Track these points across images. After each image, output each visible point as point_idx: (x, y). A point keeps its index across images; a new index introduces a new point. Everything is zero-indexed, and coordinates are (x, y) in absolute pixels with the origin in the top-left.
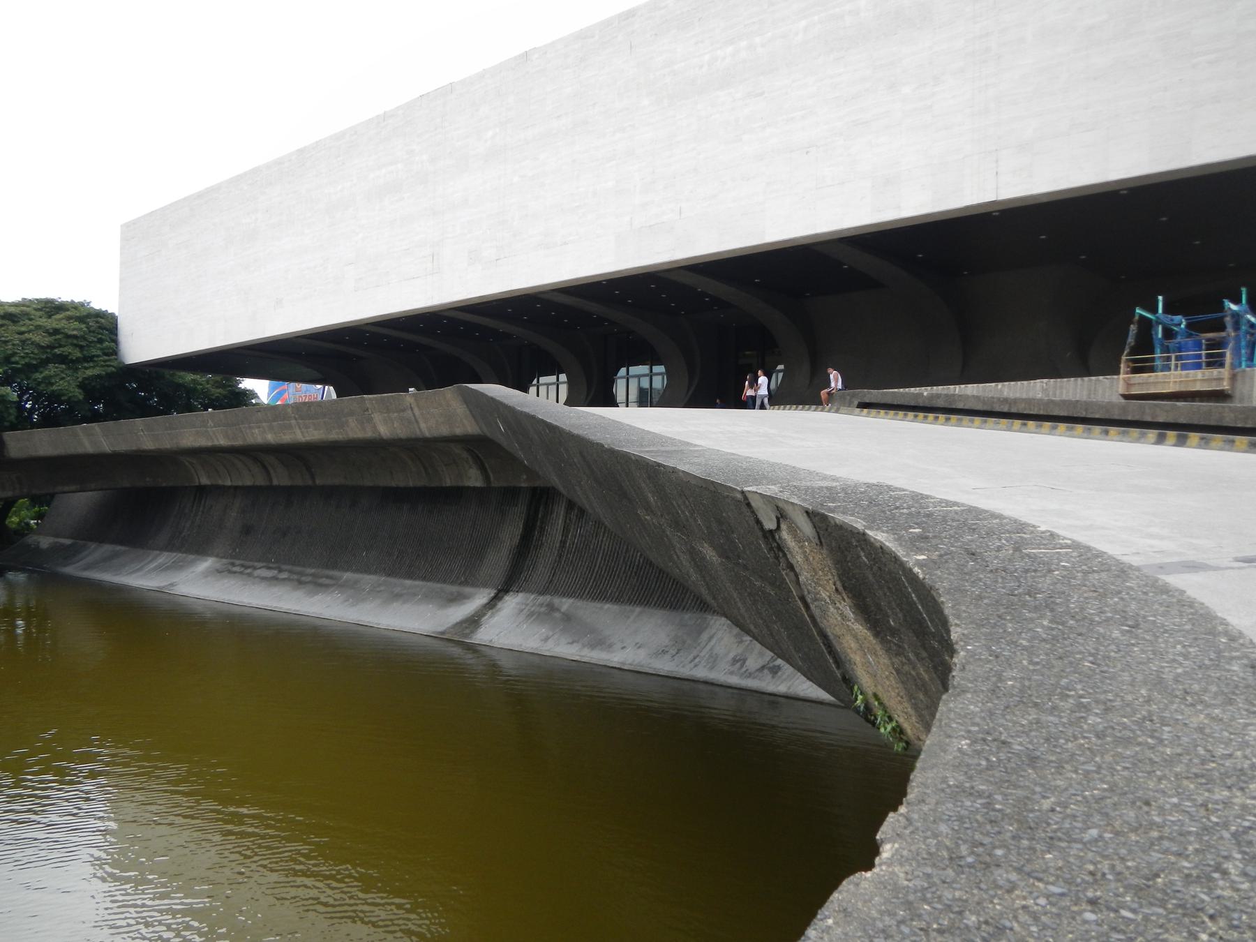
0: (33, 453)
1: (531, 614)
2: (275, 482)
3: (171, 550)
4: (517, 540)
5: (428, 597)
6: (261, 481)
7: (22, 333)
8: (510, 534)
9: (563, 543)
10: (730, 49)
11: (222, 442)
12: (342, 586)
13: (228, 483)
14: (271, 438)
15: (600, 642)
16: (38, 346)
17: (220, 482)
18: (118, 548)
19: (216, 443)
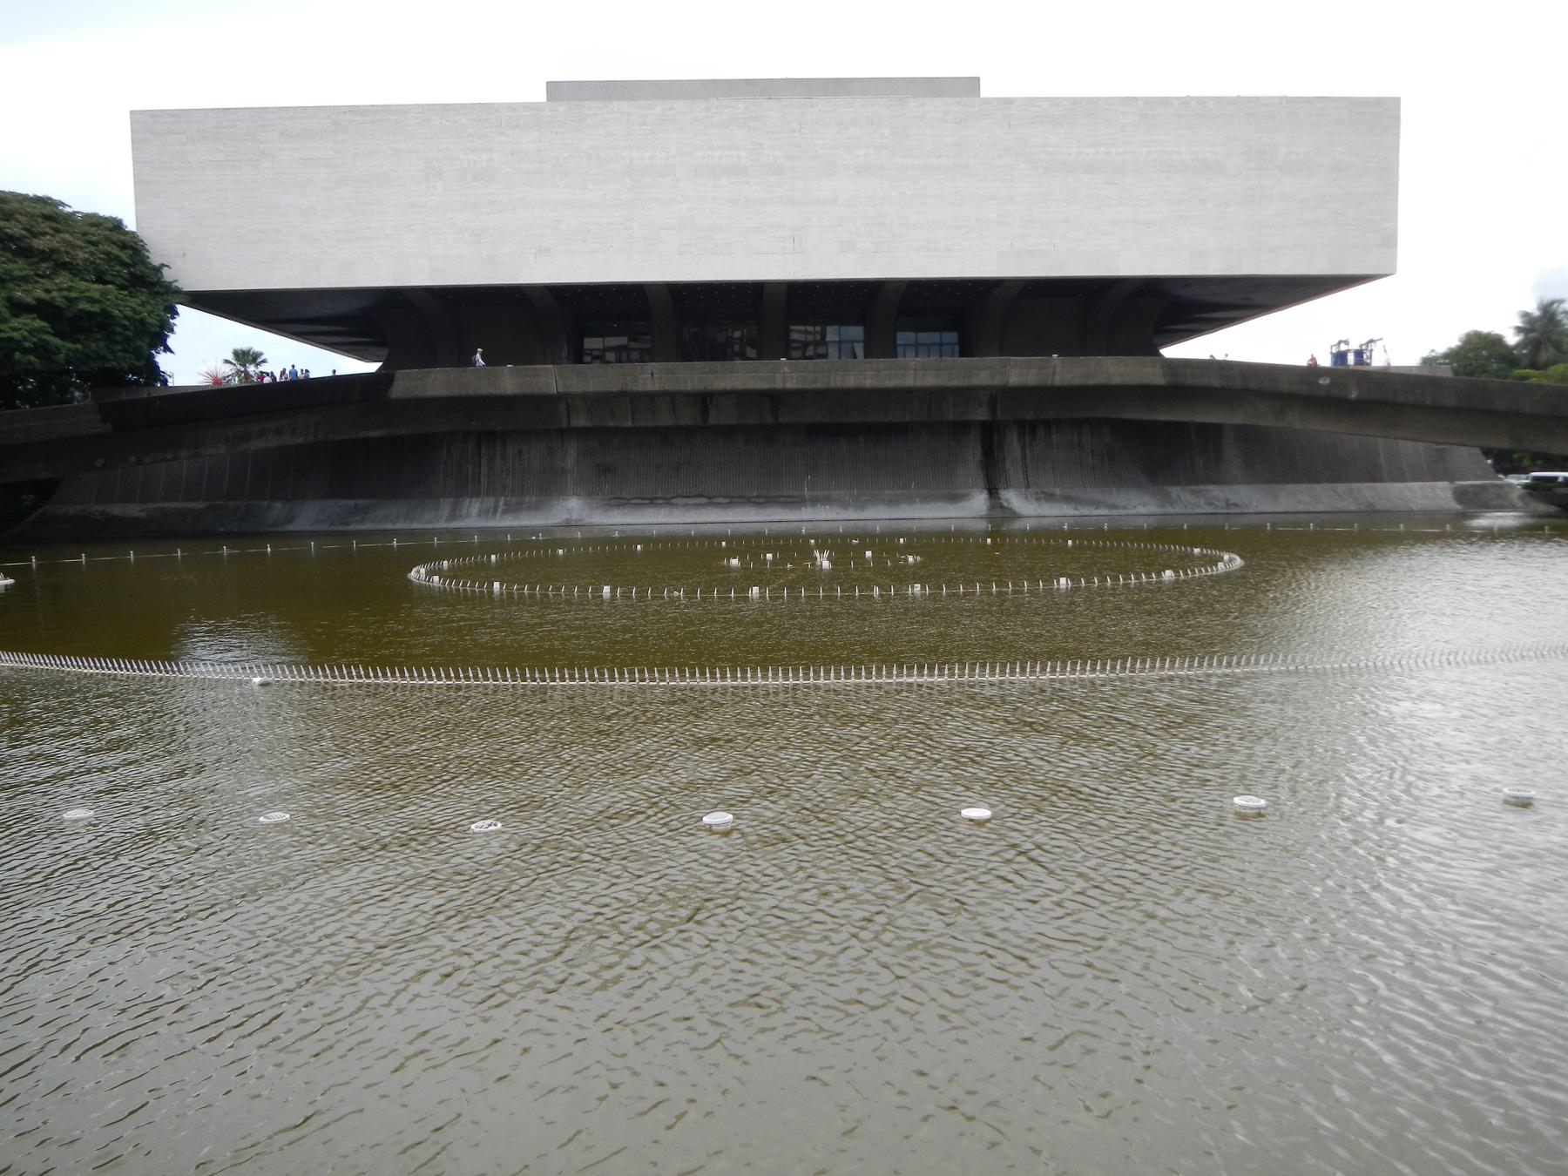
0: (419, 393)
1: (1038, 499)
2: (712, 421)
3: (476, 494)
4: (979, 456)
5: (926, 499)
6: (687, 418)
7: (93, 244)
8: (973, 453)
9: (1024, 457)
10: (1092, 150)
11: (790, 385)
12: (814, 501)
13: (629, 424)
14: (868, 383)
15: (1115, 507)
16: (123, 264)
17: (611, 424)
18: (352, 502)
19: (779, 385)
